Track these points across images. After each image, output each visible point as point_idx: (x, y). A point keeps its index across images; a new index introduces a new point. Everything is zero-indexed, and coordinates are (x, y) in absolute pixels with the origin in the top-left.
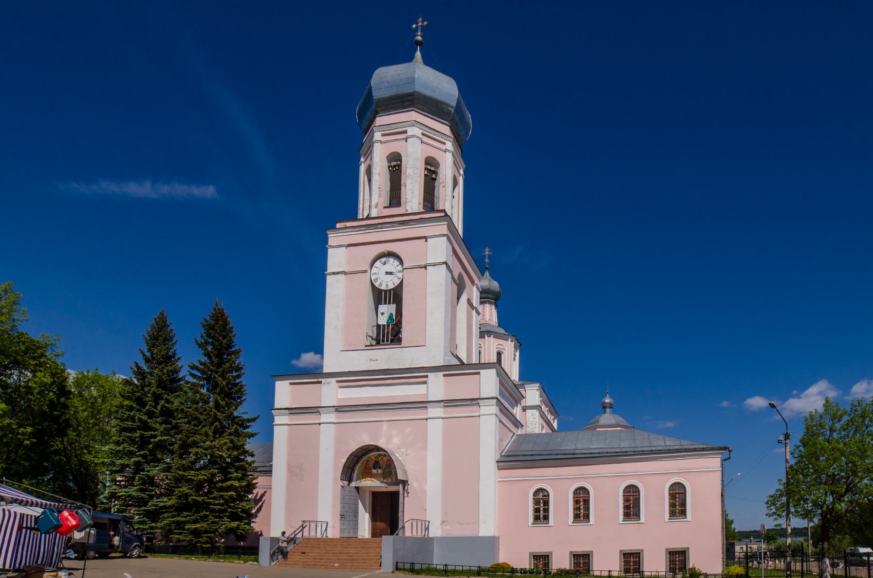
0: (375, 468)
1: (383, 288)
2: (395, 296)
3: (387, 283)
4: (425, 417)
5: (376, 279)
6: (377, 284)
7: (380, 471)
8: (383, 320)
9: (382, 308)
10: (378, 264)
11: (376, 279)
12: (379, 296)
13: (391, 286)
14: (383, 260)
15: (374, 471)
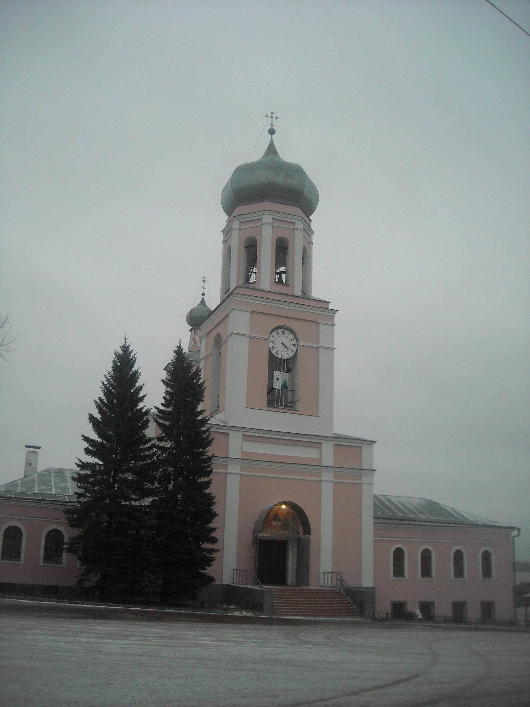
0: (275, 521)
1: (279, 356)
2: (288, 365)
3: (284, 354)
4: (319, 479)
5: (273, 348)
6: (274, 352)
7: (279, 523)
8: (277, 385)
9: (277, 374)
10: (274, 334)
11: (273, 348)
12: (275, 363)
13: (286, 357)
14: (280, 331)
15: (274, 523)
